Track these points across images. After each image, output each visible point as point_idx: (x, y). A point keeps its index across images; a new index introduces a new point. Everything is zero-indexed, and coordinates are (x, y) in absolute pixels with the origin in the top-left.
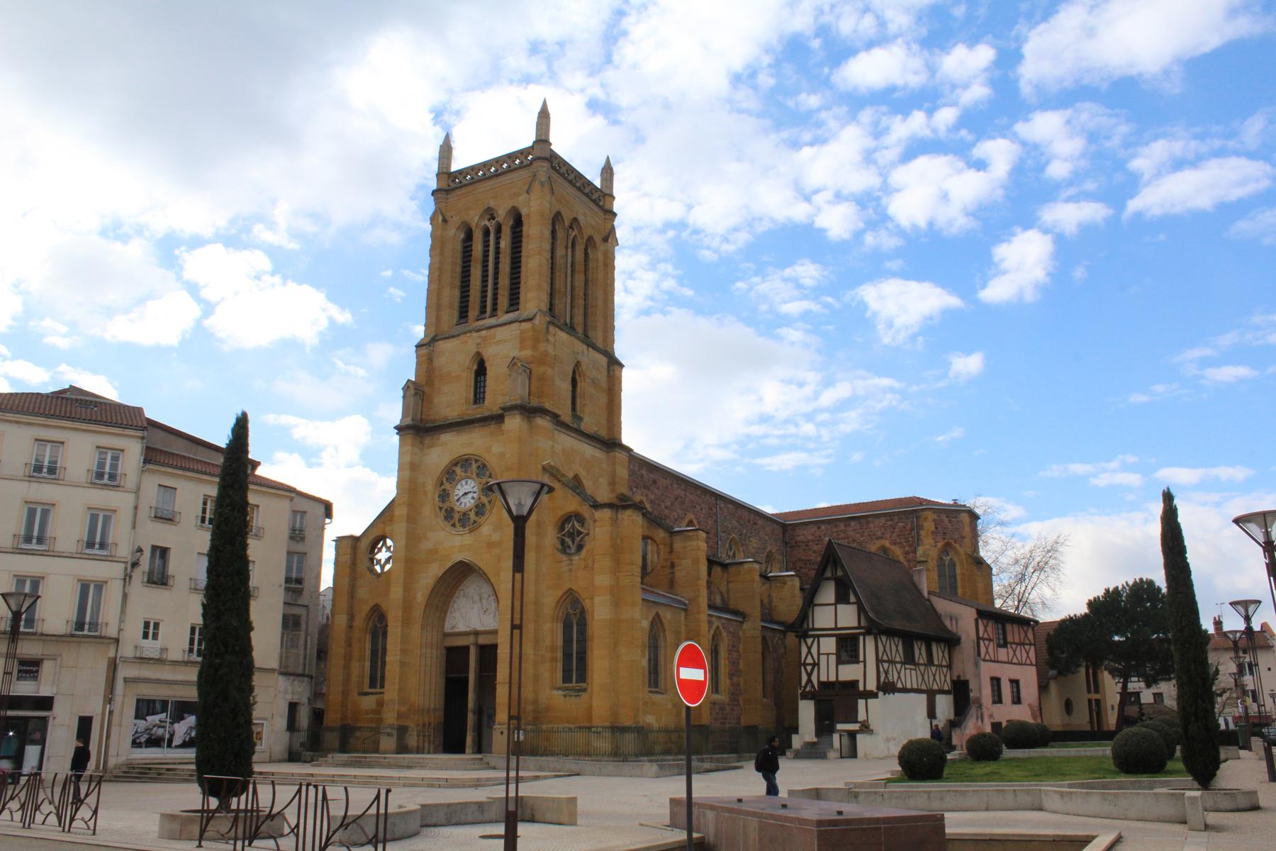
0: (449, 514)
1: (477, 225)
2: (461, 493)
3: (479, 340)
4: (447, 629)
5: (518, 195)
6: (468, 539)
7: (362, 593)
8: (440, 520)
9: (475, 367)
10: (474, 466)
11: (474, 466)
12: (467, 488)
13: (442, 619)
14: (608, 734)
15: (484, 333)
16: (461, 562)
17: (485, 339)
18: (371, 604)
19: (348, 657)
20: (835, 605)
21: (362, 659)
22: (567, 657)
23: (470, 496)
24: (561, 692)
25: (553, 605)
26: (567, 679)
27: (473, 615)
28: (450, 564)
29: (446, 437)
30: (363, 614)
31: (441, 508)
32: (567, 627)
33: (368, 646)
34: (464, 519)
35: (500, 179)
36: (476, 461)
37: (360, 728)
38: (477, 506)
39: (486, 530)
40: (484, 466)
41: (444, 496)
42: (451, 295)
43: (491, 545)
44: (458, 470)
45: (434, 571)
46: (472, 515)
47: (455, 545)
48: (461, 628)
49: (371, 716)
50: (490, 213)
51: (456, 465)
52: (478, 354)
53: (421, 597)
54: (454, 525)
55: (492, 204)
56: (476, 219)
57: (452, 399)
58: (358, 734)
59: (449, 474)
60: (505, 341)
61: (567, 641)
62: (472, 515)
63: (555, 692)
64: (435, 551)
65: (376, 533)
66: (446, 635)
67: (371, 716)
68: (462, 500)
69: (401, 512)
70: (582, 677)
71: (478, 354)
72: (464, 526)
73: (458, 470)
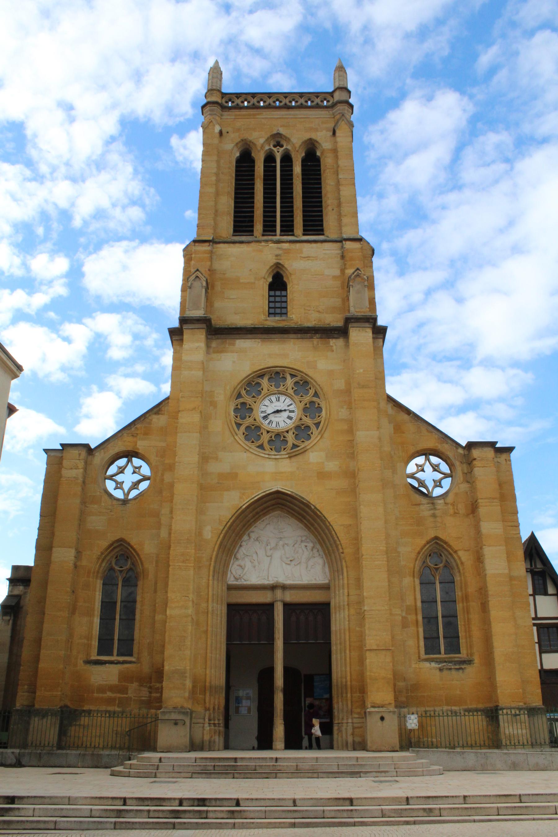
0: (253, 433)
1: (262, 146)
2: (270, 411)
3: (280, 252)
4: (231, 581)
5: (316, 130)
6: (286, 465)
7: (96, 522)
8: (240, 437)
9: (270, 280)
10: (290, 382)
11: (290, 382)
12: (280, 405)
13: (226, 565)
14: (524, 717)
15: (286, 246)
16: (278, 492)
17: (287, 251)
18: (112, 537)
19: (73, 609)
20: (534, 595)
21: (89, 613)
22: (430, 620)
23: (285, 414)
24: (433, 665)
25: (413, 555)
26: (431, 646)
27: (278, 563)
28: (258, 493)
29: (242, 344)
30: (97, 552)
31: (239, 425)
32: (426, 584)
33: (98, 597)
34: (278, 440)
35: (292, 112)
36: (292, 376)
37: (89, 712)
38: (297, 428)
39: (316, 455)
40: (306, 383)
41: (243, 410)
42: (227, 203)
43: (322, 475)
44: (265, 382)
45: (232, 502)
46: (290, 438)
47: (271, 473)
48: (254, 579)
49: (109, 694)
50: (278, 139)
51: (262, 376)
52: (278, 265)
53: (211, 533)
54: (261, 447)
55: (282, 131)
56: (262, 141)
57: (246, 305)
58: (84, 720)
59: (253, 384)
60: (316, 258)
61: (428, 602)
62: (290, 438)
63: (427, 665)
64: (233, 476)
65: (120, 447)
66: (230, 588)
67: (109, 694)
68: (271, 417)
69: (189, 418)
70: (453, 645)
71: (278, 265)
72: (278, 450)
73: (265, 382)
